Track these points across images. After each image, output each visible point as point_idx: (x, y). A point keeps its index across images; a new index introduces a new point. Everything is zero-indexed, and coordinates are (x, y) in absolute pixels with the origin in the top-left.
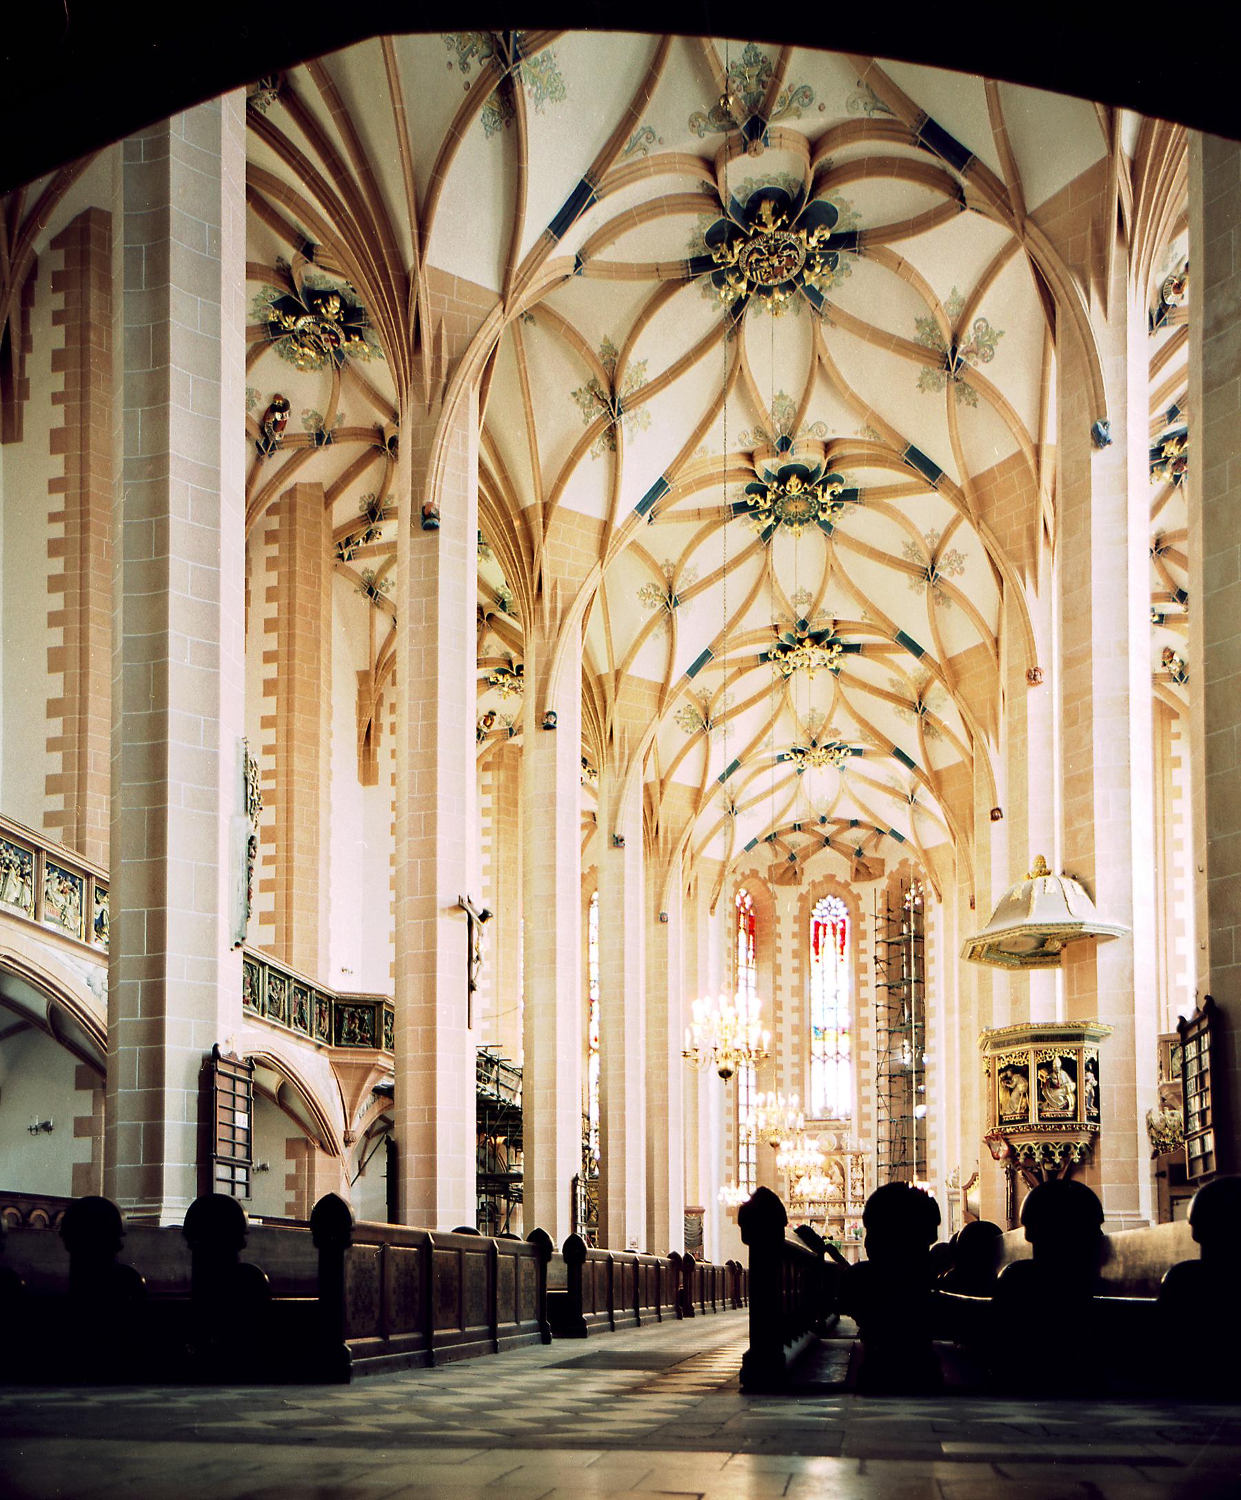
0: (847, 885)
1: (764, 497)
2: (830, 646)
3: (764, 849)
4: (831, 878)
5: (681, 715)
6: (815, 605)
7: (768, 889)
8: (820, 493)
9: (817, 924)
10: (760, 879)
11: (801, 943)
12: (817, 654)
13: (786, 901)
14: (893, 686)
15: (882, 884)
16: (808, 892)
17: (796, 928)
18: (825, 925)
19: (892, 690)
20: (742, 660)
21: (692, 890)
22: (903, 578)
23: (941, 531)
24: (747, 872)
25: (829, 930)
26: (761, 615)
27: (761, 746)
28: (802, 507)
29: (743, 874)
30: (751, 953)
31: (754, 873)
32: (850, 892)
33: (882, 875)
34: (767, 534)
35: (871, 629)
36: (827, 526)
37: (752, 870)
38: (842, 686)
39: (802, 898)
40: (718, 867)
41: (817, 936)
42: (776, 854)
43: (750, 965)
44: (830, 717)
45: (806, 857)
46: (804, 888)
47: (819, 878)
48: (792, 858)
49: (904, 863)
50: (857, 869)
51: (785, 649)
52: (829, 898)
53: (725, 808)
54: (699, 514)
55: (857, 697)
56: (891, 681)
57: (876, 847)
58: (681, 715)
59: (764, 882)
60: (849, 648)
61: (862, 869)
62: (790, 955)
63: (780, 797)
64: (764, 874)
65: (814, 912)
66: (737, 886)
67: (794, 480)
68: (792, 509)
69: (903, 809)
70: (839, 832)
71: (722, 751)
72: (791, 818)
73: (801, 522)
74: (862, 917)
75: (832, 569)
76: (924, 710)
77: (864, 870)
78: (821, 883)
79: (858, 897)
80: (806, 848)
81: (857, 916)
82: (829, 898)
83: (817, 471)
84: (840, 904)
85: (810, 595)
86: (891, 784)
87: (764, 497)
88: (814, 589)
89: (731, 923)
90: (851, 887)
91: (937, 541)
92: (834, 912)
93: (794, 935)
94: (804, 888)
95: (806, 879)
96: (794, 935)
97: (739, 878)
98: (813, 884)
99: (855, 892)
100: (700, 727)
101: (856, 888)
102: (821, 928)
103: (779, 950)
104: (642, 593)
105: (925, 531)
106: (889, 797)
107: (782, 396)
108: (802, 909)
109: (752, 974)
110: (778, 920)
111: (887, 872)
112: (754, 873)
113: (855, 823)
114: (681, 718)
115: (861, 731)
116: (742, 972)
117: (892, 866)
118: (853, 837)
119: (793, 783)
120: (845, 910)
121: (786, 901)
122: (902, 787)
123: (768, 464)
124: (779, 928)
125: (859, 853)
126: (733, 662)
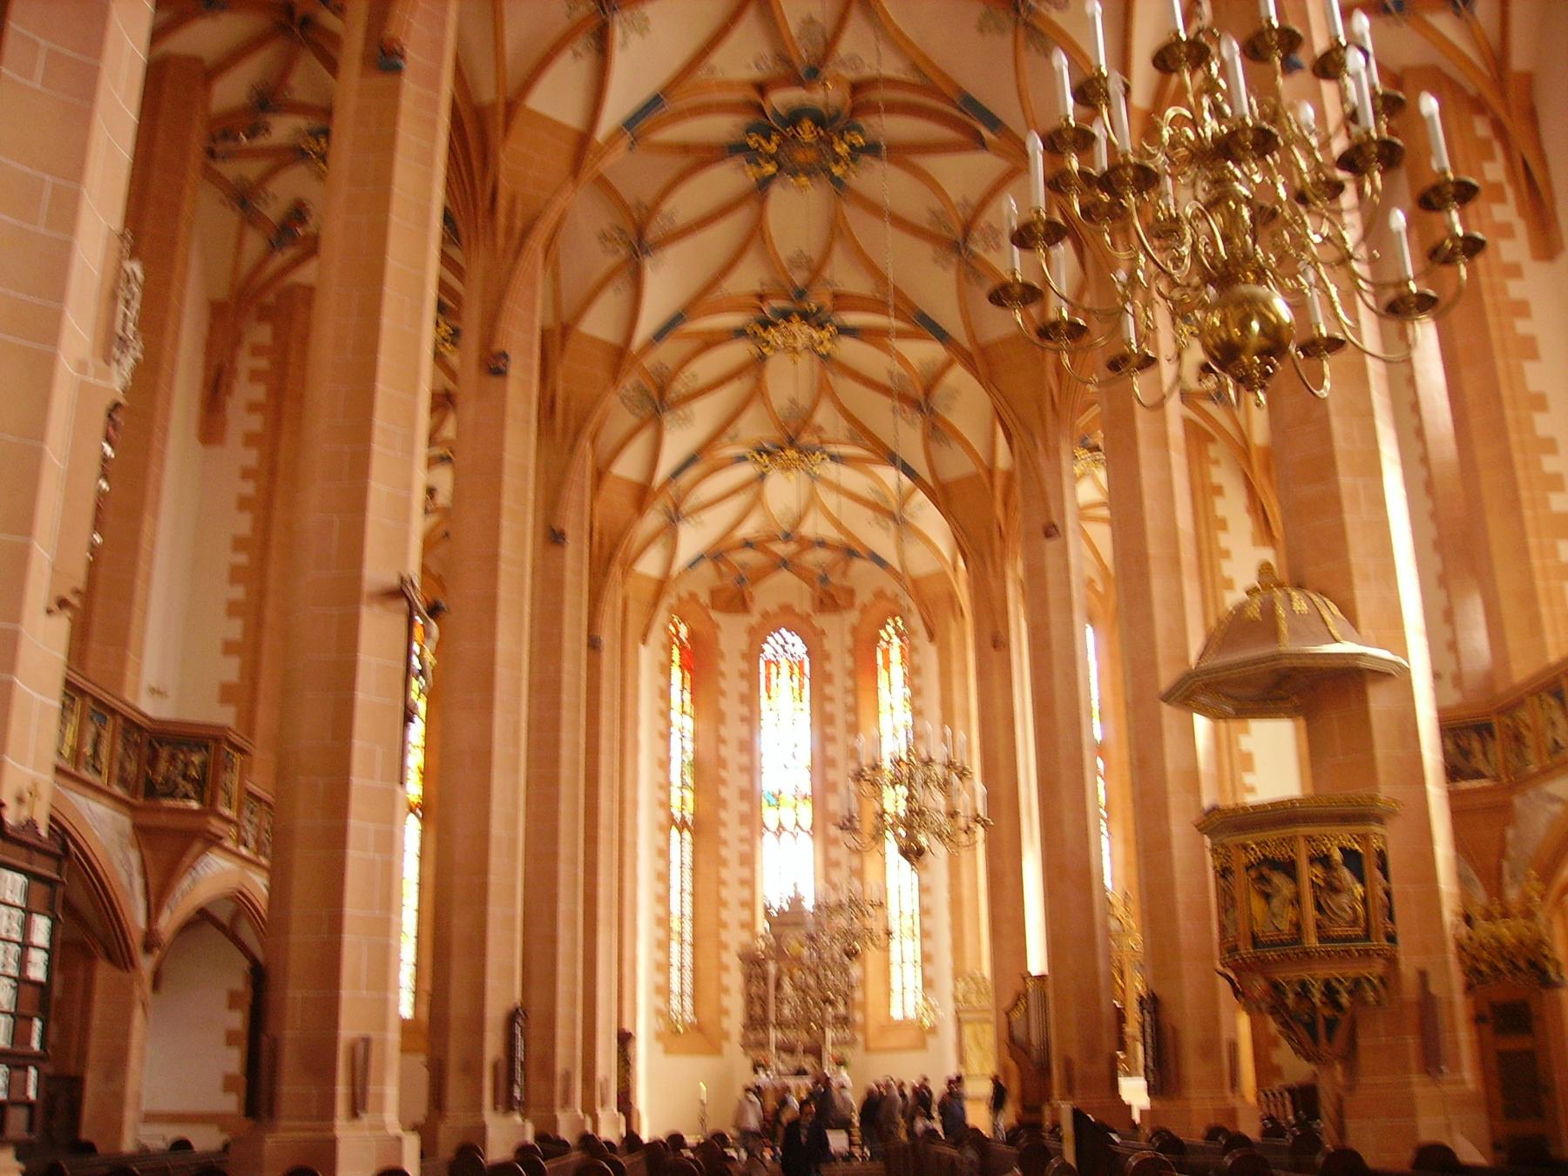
1: (769, 141)
2: (821, 326)
3: (706, 568)
6: (816, 272)
7: (710, 618)
8: (836, 139)
9: (768, 663)
12: (802, 332)
13: (731, 632)
15: (852, 617)
17: (744, 666)
18: (777, 664)
20: (711, 332)
22: (925, 250)
23: (974, 198)
24: (684, 594)
26: (747, 278)
27: (725, 439)
28: (811, 155)
30: (687, 696)
31: (693, 597)
32: (812, 626)
33: (850, 605)
34: (764, 184)
35: (879, 306)
36: (838, 182)
40: (652, 588)
41: (768, 678)
42: (720, 574)
46: (754, 618)
47: (772, 607)
48: (741, 580)
49: (880, 595)
50: (822, 602)
51: (766, 324)
54: (685, 148)
55: (849, 390)
56: (890, 373)
57: (844, 574)
60: (846, 331)
61: (827, 600)
64: (704, 598)
66: (672, 610)
67: (807, 125)
68: (800, 157)
69: (887, 529)
70: (800, 552)
71: (678, 442)
72: (748, 530)
73: (808, 174)
74: (827, 656)
75: (837, 230)
76: (932, 411)
77: (830, 599)
81: (816, 653)
83: (838, 113)
84: (797, 640)
85: (810, 260)
86: (872, 497)
87: (769, 141)
88: (813, 251)
89: (662, 656)
91: (969, 211)
93: (742, 675)
94: (754, 618)
98: (765, 615)
101: (821, 621)
102: (773, 666)
103: (722, 693)
104: (604, 237)
105: (955, 197)
106: (869, 513)
107: (809, 22)
108: (751, 644)
109: (689, 724)
112: (693, 597)
113: (822, 544)
115: (850, 431)
116: (675, 715)
117: (864, 596)
118: (819, 556)
119: (755, 487)
121: (731, 632)
123: (782, 99)
124: (724, 666)
125: (824, 580)
126: (698, 334)
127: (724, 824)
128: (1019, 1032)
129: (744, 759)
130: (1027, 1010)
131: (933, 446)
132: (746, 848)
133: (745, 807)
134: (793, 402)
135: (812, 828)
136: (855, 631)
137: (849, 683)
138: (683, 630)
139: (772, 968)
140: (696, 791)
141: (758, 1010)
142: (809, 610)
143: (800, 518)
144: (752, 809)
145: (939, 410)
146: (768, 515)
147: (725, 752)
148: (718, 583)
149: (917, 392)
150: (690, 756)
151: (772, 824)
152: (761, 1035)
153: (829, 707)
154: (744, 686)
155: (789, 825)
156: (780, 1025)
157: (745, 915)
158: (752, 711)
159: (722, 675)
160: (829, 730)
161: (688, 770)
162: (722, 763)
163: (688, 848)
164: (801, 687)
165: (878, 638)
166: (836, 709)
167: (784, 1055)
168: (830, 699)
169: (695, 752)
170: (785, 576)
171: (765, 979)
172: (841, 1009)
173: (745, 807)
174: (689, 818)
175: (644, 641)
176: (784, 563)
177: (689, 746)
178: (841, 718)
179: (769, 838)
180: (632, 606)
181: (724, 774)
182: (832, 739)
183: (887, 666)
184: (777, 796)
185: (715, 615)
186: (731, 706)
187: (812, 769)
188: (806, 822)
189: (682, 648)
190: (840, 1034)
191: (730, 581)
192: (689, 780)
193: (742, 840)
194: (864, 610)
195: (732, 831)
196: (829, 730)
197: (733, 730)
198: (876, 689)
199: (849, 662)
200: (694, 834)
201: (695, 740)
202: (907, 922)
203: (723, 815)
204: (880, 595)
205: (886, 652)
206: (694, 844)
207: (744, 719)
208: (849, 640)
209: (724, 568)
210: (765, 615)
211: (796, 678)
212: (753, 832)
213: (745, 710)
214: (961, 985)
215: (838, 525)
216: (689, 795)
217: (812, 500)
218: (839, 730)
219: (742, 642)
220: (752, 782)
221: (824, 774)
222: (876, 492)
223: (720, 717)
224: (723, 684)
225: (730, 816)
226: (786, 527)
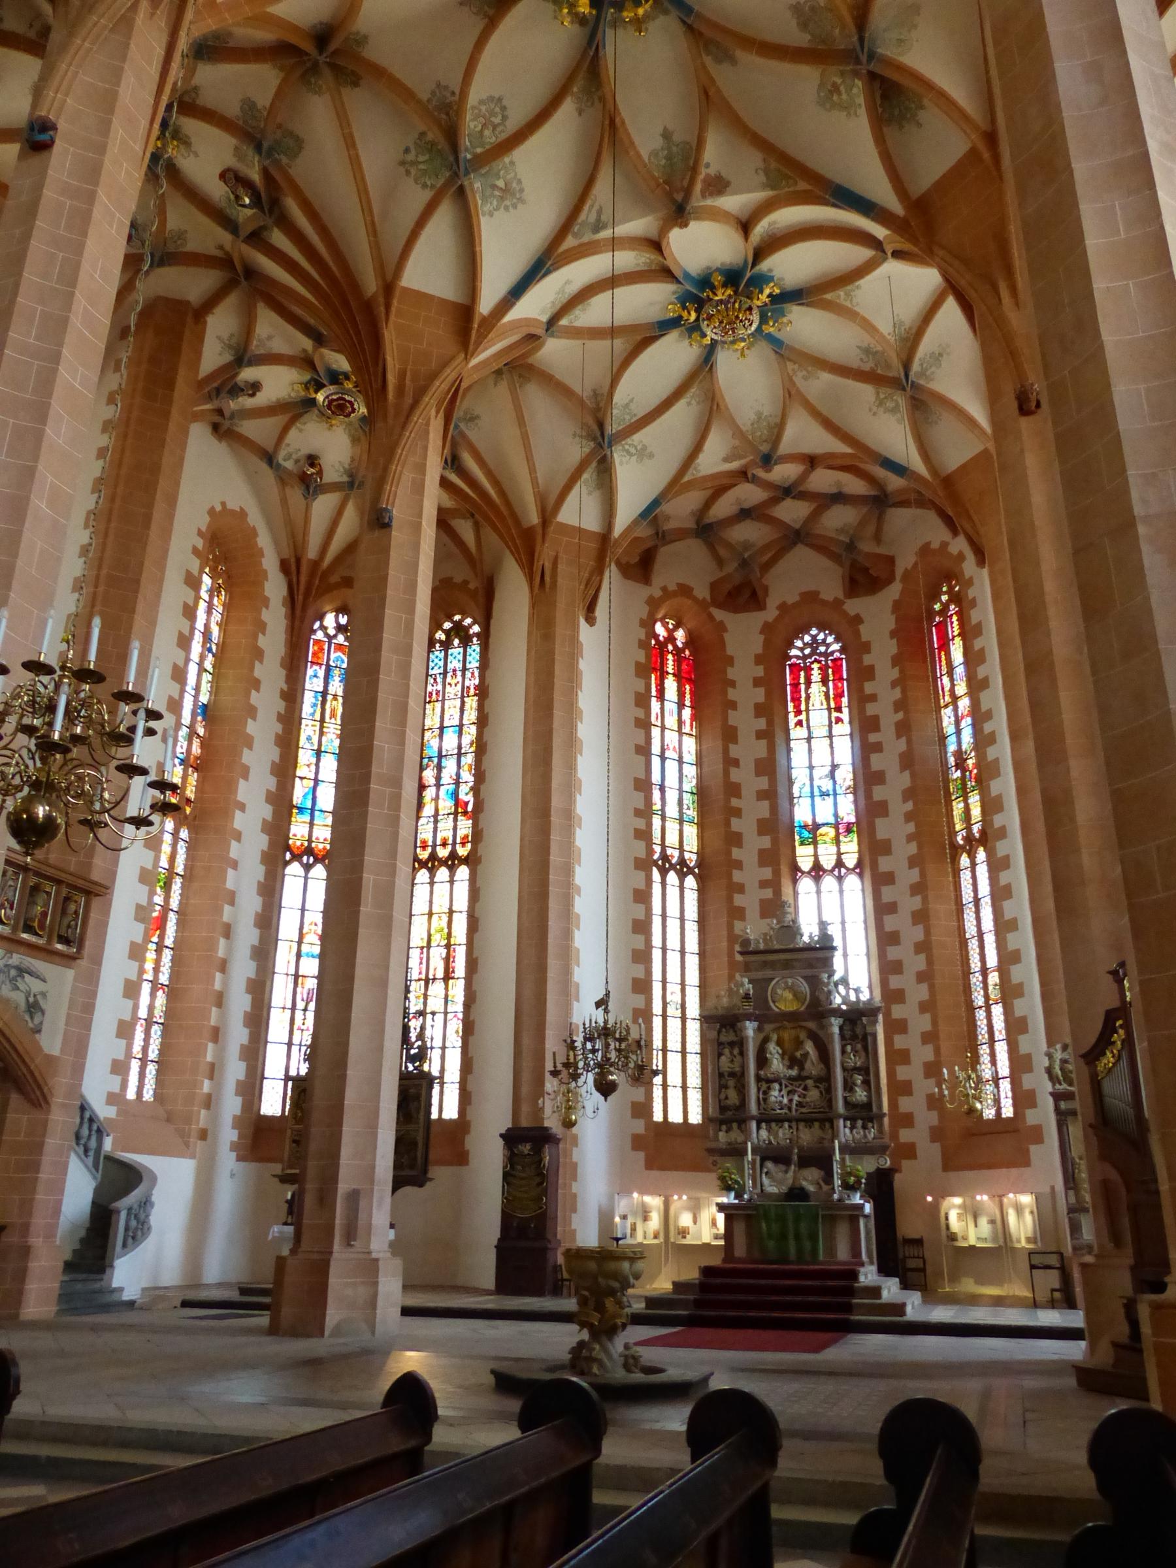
0: (837, 604)
4: (810, 597)
5: (411, 157)
7: (711, 617)
10: (695, 599)
11: (768, 694)
14: (804, 25)
15: (894, 591)
16: (777, 619)
17: (760, 671)
18: (809, 670)
19: (802, 39)
21: (547, 578)
24: (672, 587)
25: (816, 675)
29: (664, 589)
30: (687, 713)
31: (685, 590)
32: (845, 613)
33: (890, 580)
37: (680, 585)
38: (708, 60)
39: (767, 628)
40: (593, 545)
41: (795, 686)
42: (720, 562)
43: (687, 729)
44: (701, 142)
45: (767, 567)
46: (770, 613)
47: (792, 598)
48: (744, 564)
49: (925, 550)
52: (814, 631)
53: (594, 439)
57: (878, 538)
58: (411, 157)
59: (702, 604)
62: (752, 712)
63: (683, 414)
65: (794, 652)
69: (894, 410)
76: (872, 56)
78: (795, 605)
79: (858, 620)
80: (766, 547)
81: (854, 647)
82: (814, 631)
84: (830, 639)
86: (867, 367)
90: (845, 607)
92: (822, 649)
93: (757, 682)
94: (770, 613)
95: (773, 602)
96: (757, 682)
97: (658, 593)
98: (783, 607)
99: (852, 613)
100: (448, 174)
101: (853, 606)
102: (802, 674)
108: (767, 644)
109: (690, 745)
110: (730, 661)
111: (899, 572)
113: (839, 498)
114: (414, 163)
117: (905, 561)
118: (838, 519)
120: (836, 647)
122: (888, 366)
125: (851, 547)
127: (739, 865)
128: (1117, 1090)
129: (763, 783)
130: (1129, 1042)
131: (889, 132)
132: (768, 893)
133: (766, 842)
134: (666, 135)
135: (859, 864)
136: (897, 606)
137: (895, 673)
138: (680, 635)
139: (750, 1028)
140: (702, 826)
141: (733, 1097)
142: (840, 595)
143: (780, 427)
144: (775, 842)
145: (887, 50)
146: (738, 432)
147: (735, 775)
148: (720, 575)
149: (843, 37)
150: (690, 784)
151: (805, 864)
152: (736, 1136)
153: (871, 709)
154: (759, 695)
155: (828, 862)
156: (767, 1119)
157: (900, 1042)
158: (770, 723)
159: (733, 684)
160: (873, 738)
161: (688, 799)
162: (733, 790)
163: (691, 898)
164: (838, 696)
165: (931, 614)
166: (884, 709)
167: (769, 1165)
168: (873, 698)
169: (700, 778)
170: (802, 555)
171: (740, 1044)
172: (860, 1095)
173: (766, 842)
174: (691, 858)
175: (591, 620)
176: (795, 537)
177: (690, 771)
178: (889, 719)
179: (806, 885)
180: (561, 567)
181: (735, 802)
182: (878, 748)
183: (945, 645)
184: (816, 826)
185: (719, 614)
186: (745, 721)
187: (855, 790)
188: (851, 861)
189: (678, 652)
190: (859, 1133)
191: (731, 567)
192: (691, 813)
193: (763, 884)
194: (906, 576)
195: (751, 874)
196: (873, 738)
197: (749, 749)
198: (935, 679)
199: (892, 647)
200: (700, 879)
201: (699, 763)
202: (994, 978)
203: (736, 853)
204: (925, 550)
205: (942, 629)
206: (701, 891)
207: (760, 735)
208: (890, 623)
209: (722, 552)
210: (783, 607)
211: (831, 684)
212: (777, 874)
213: (762, 724)
214: (1058, 1055)
215: (829, 425)
216: (691, 832)
217: (791, 395)
218: (886, 734)
219: (757, 644)
220: (774, 809)
221: (868, 795)
222: (867, 351)
223: (730, 735)
224: (732, 694)
225: (747, 854)
226: (765, 448)
